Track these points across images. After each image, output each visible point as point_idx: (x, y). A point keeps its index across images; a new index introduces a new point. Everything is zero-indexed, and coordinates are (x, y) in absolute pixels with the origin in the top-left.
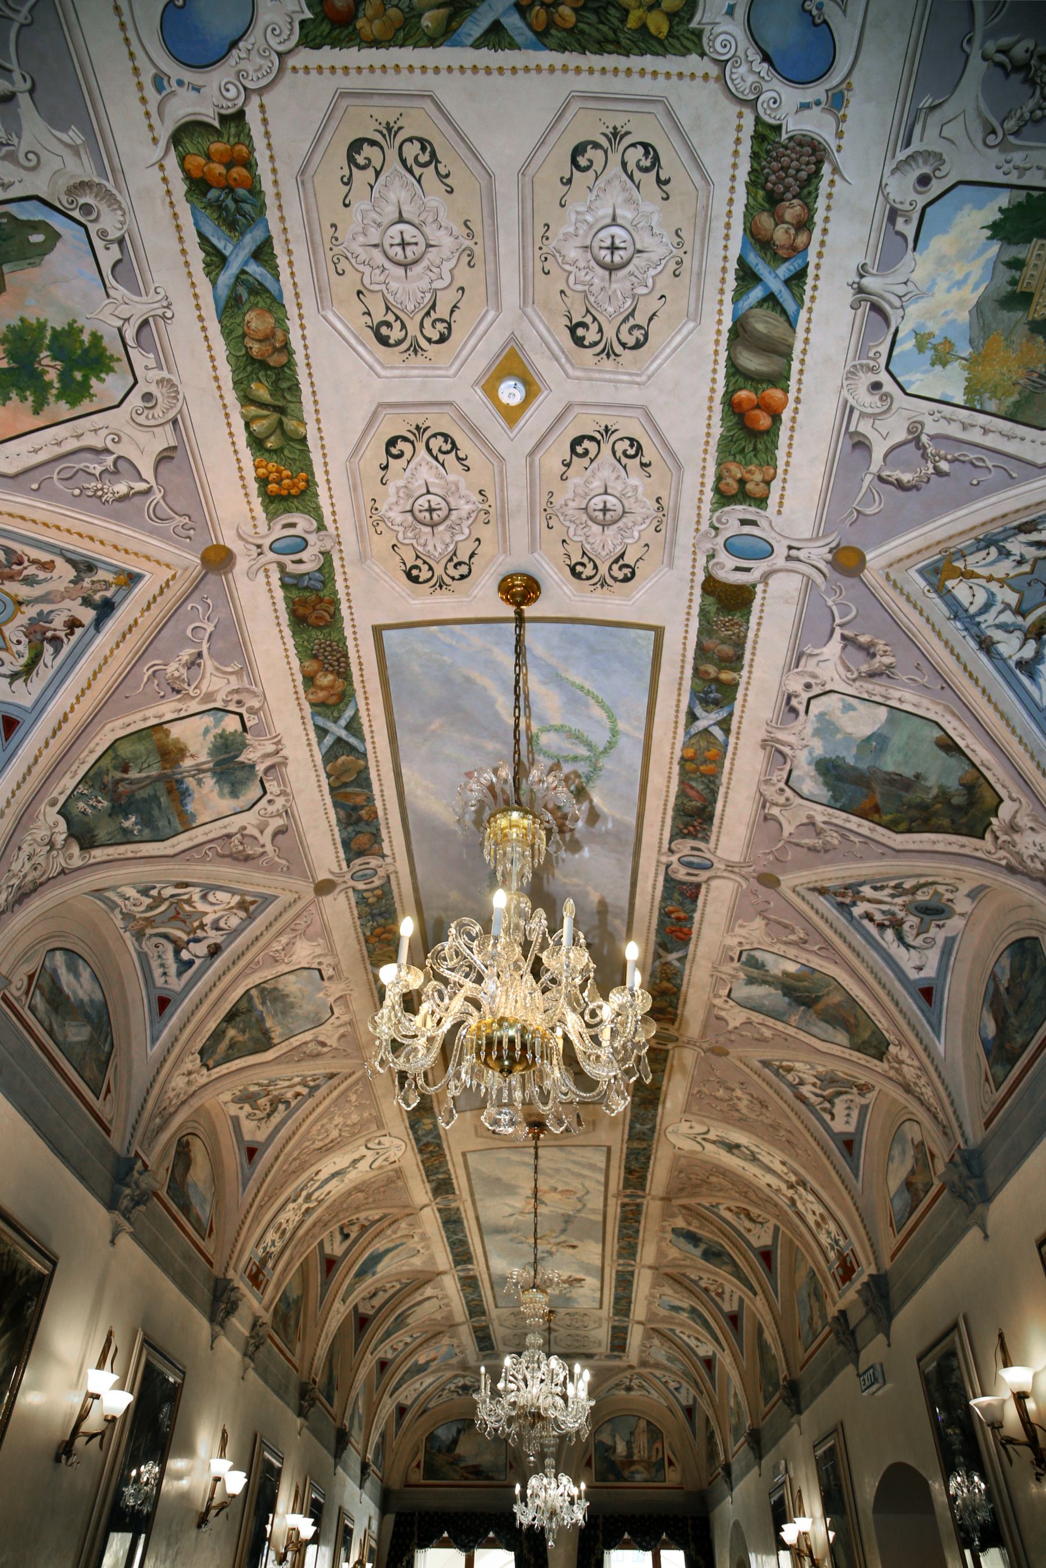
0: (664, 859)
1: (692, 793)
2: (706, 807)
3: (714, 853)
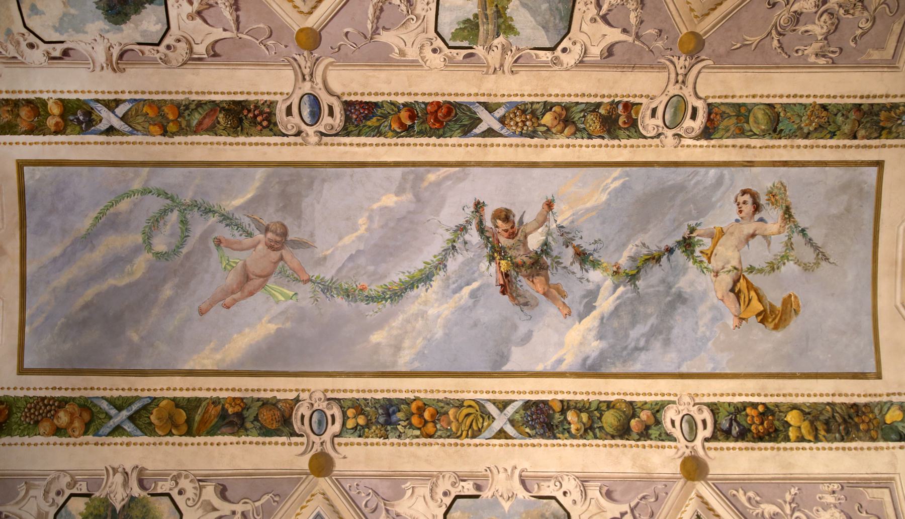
0: (314, 139)
1: (208, 122)
2: (223, 109)
3: (290, 95)
